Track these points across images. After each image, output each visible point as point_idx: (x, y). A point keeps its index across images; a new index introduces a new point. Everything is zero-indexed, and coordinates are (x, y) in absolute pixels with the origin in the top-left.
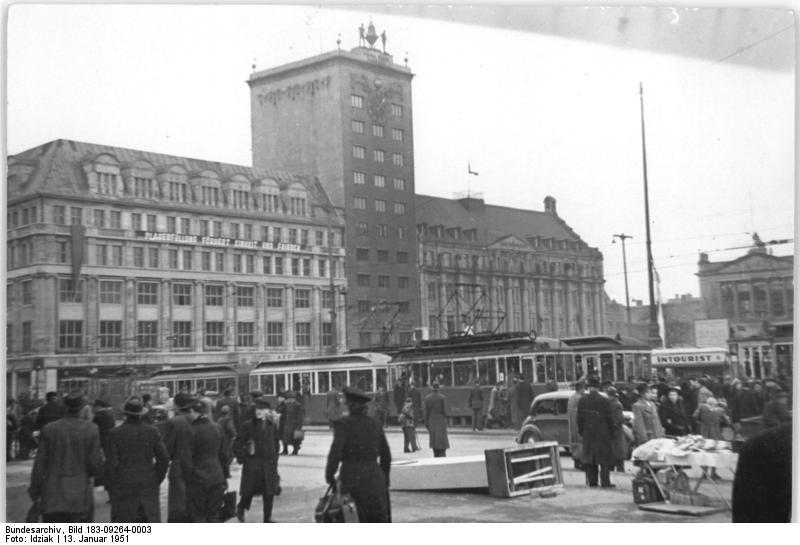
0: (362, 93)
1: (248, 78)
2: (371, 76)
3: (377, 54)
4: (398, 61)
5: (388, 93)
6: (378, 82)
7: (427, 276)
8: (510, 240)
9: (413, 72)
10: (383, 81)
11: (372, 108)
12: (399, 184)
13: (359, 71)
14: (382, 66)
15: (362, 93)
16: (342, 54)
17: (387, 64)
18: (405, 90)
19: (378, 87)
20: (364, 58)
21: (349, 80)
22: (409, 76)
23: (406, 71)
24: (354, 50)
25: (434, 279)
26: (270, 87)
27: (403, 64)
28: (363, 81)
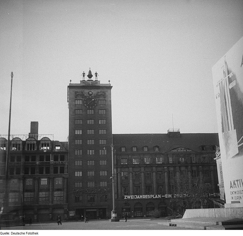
0: (81, 98)
2: (86, 91)
3: (91, 82)
5: (97, 96)
11: (86, 103)
12: (101, 132)
13: (78, 90)
14: (95, 86)
15: (81, 98)
16: (71, 85)
17: (98, 85)
18: (107, 93)
20: (82, 85)
21: (74, 94)
22: (110, 87)
23: (108, 86)
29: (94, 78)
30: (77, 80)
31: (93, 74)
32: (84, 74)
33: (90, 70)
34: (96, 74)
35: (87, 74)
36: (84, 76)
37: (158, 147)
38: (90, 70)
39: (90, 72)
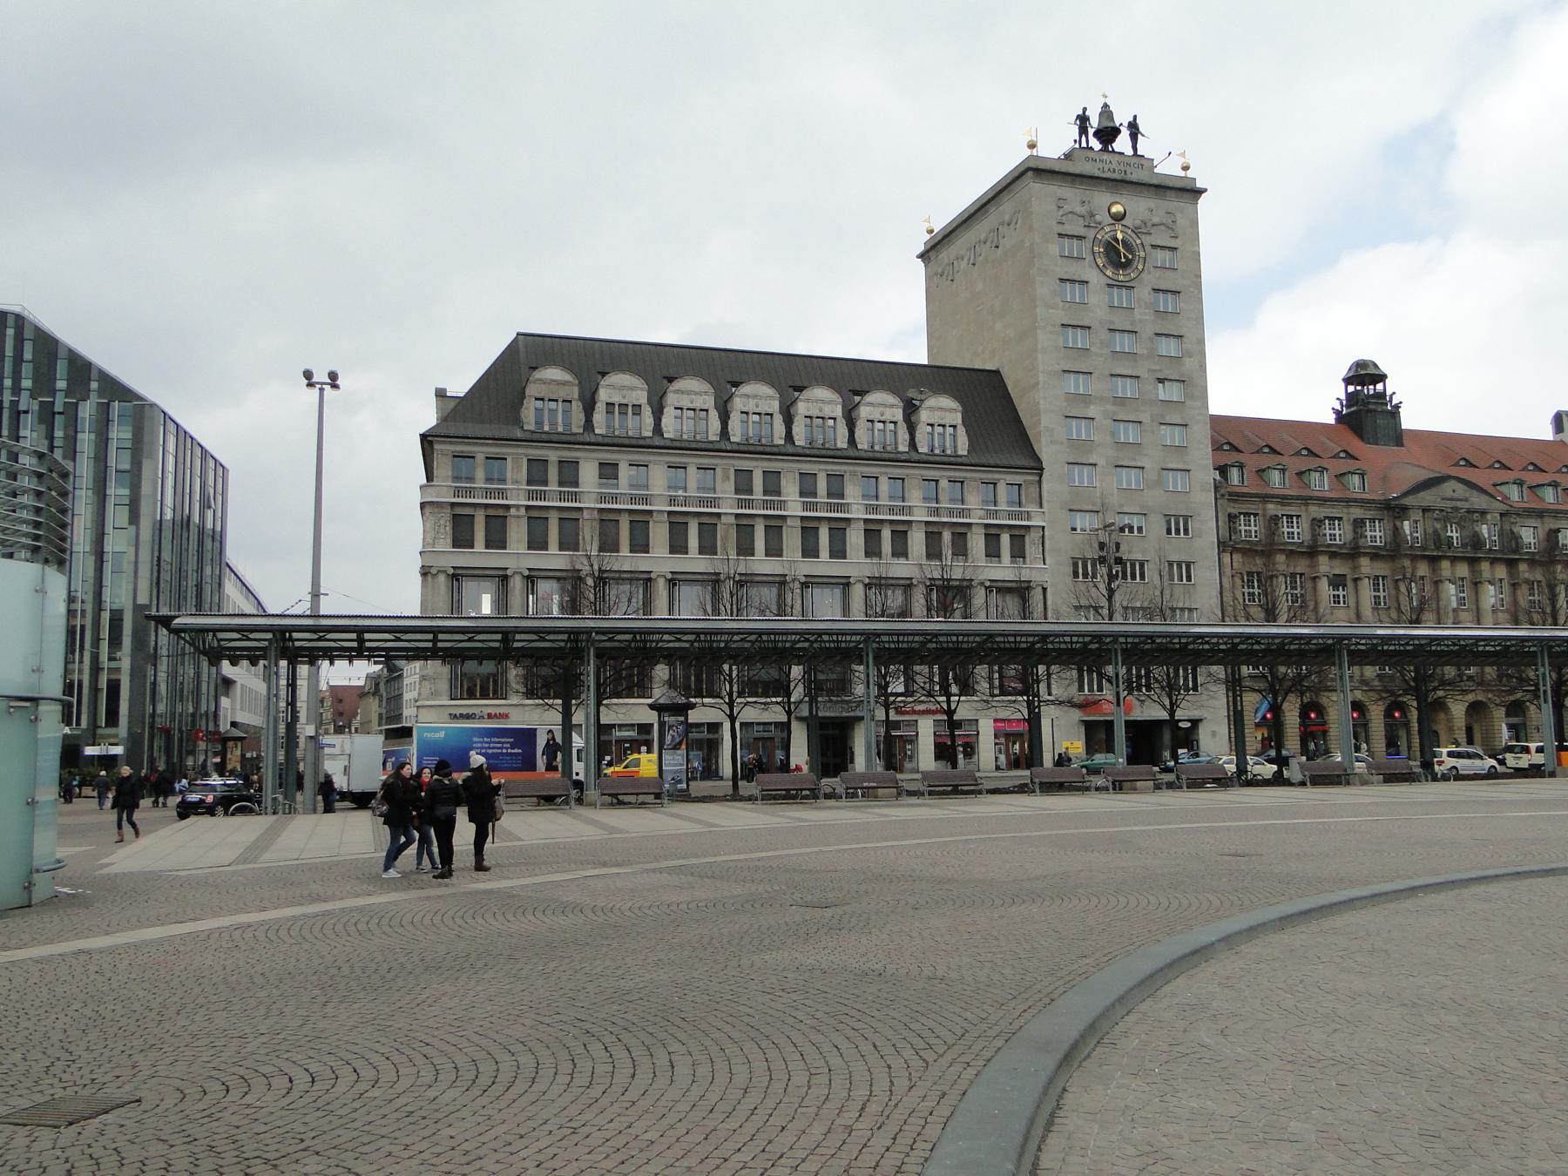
1: (922, 248)
3: (1117, 158)
4: (1168, 168)
6: (1116, 209)
7: (1237, 557)
8: (1448, 488)
9: (1199, 185)
10: (1137, 207)
15: (1082, 232)
18: (1181, 221)
19: (1119, 218)
21: (1054, 207)
24: (1068, 156)
25: (1258, 564)
26: (945, 255)
27: (1182, 174)
28: (1080, 210)
29: (1122, 144)
30: (1057, 142)
31: (1121, 119)
32: (1083, 120)
33: (1106, 105)
34: (1134, 128)
35: (1094, 122)
36: (1083, 130)
37: (1362, 475)
38: (1106, 105)
39: (1106, 112)
